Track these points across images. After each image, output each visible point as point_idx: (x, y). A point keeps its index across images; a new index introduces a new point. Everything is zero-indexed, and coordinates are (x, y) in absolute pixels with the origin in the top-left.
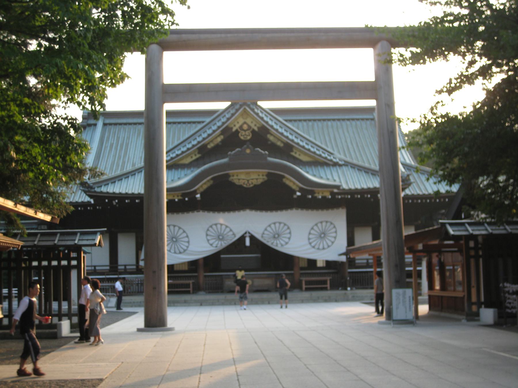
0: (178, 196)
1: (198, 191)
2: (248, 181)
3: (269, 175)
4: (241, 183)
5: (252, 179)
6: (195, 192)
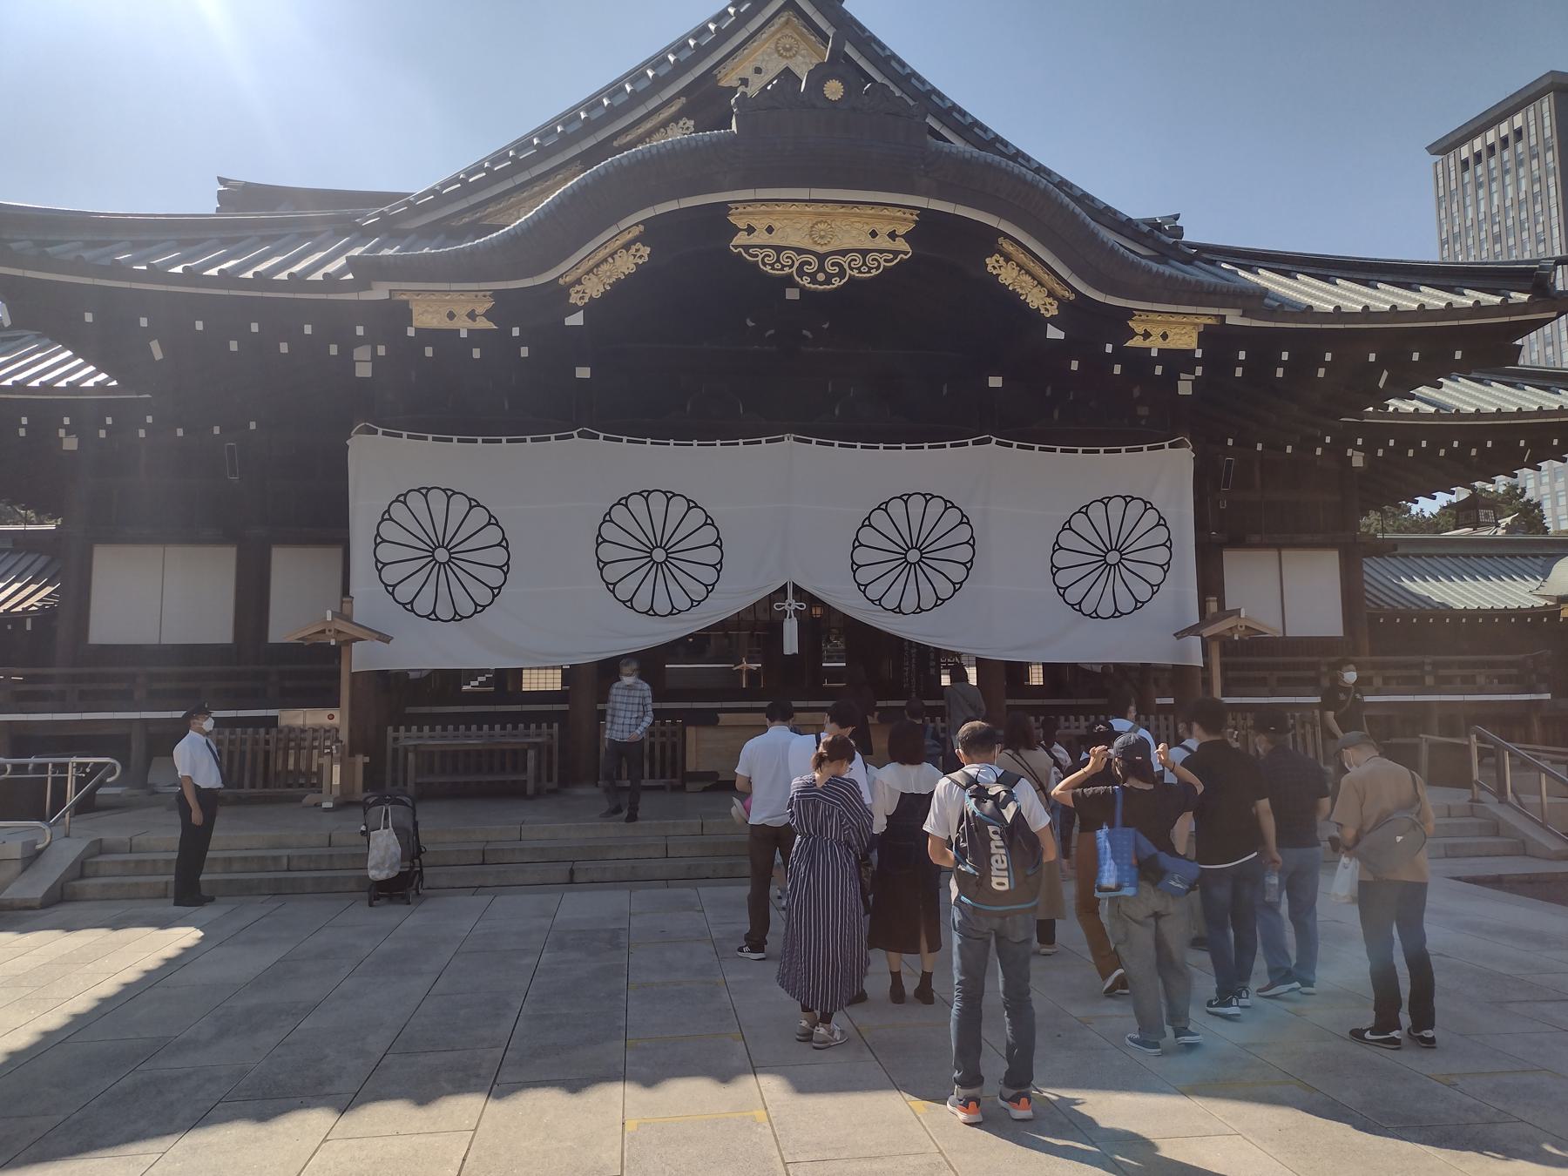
0: (472, 316)
1: (574, 299)
2: (822, 258)
3: (928, 227)
4: (786, 266)
5: (844, 253)
6: (557, 295)
